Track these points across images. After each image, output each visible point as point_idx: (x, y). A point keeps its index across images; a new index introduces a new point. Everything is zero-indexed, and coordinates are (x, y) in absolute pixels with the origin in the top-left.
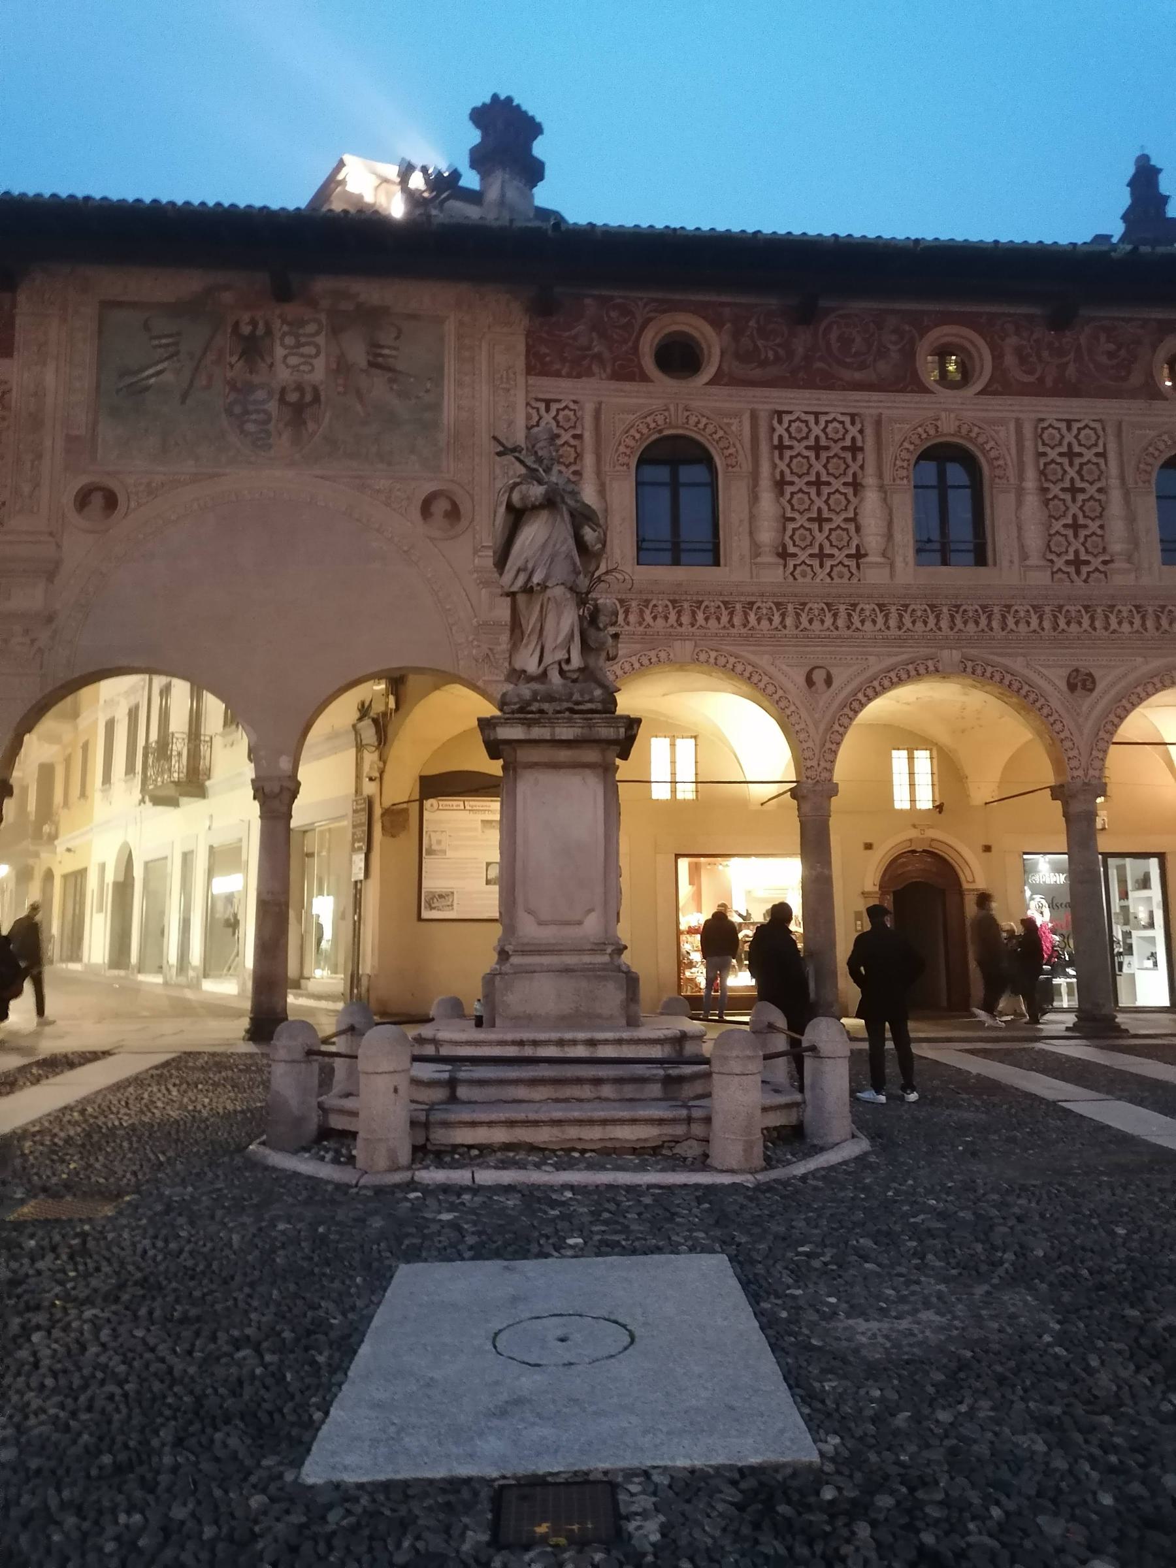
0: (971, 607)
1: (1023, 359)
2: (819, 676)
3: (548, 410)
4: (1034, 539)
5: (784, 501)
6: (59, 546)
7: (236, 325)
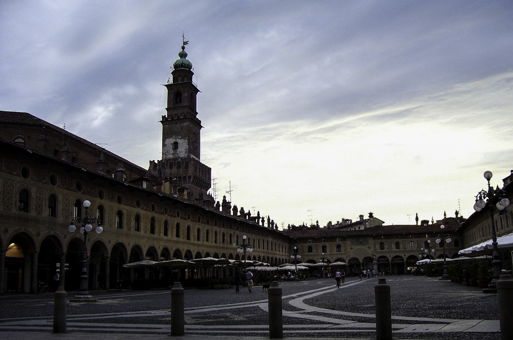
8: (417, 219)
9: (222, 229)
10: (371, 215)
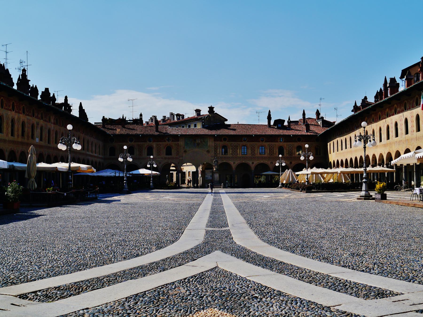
4: (250, 153)
8: (269, 118)
9: (21, 115)
10: (211, 109)
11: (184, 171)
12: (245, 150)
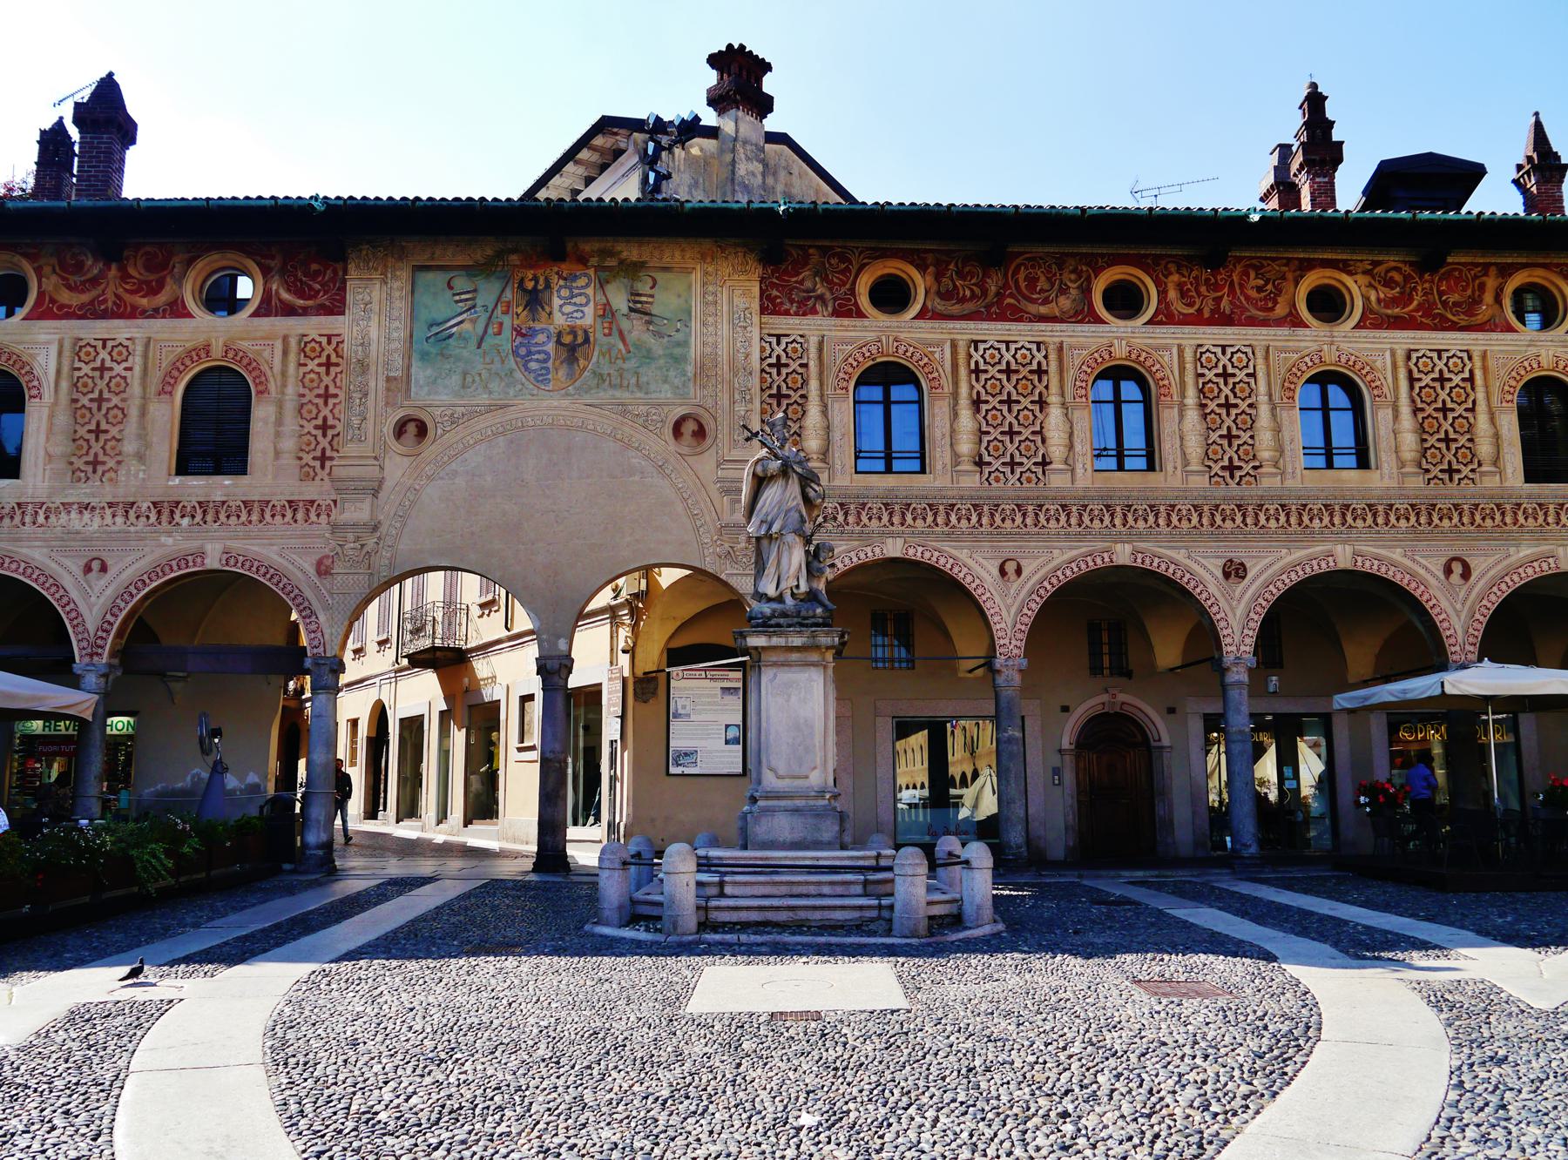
0: (1141, 507)
1: (1183, 294)
2: (1011, 567)
3: (778, 343)
4: (1194, 447)
5: (980, 417)
6: (382, 468)
7: (522, 281)
10: (740, 77)
11: (490, 693)
12: (1133, 416)
